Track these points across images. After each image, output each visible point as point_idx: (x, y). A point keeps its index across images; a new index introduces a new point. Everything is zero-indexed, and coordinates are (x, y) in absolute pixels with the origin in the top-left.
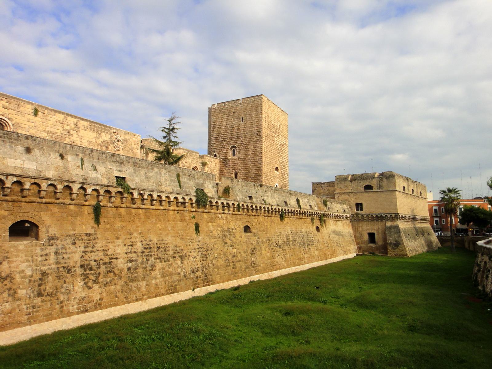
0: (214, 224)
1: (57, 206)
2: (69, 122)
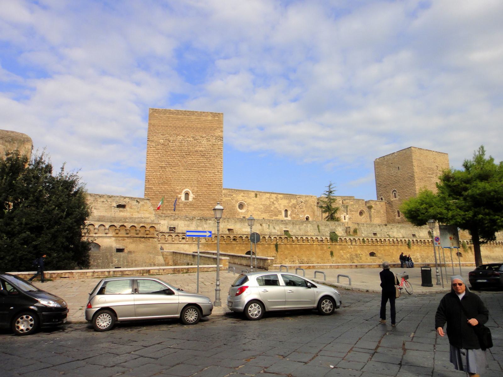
0: (344, 251)
1: (261, 245)
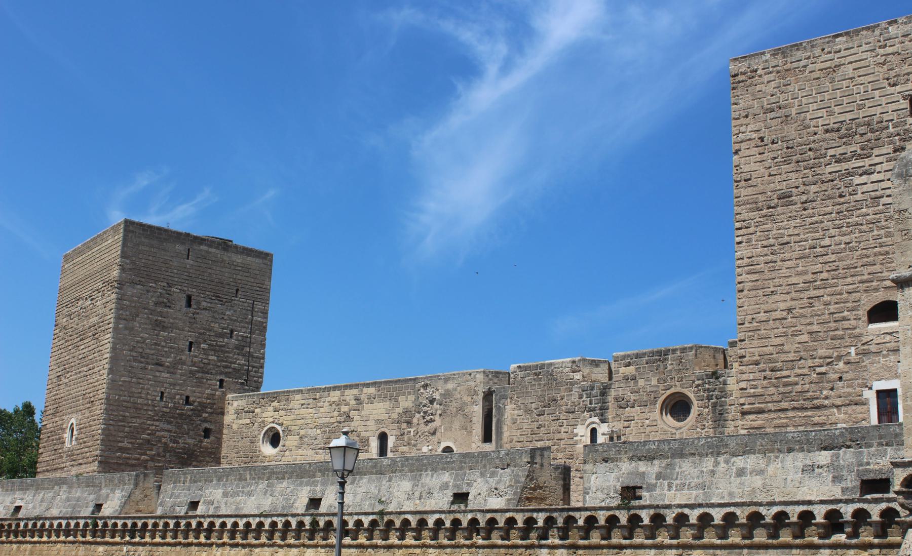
2: (348, 398)
